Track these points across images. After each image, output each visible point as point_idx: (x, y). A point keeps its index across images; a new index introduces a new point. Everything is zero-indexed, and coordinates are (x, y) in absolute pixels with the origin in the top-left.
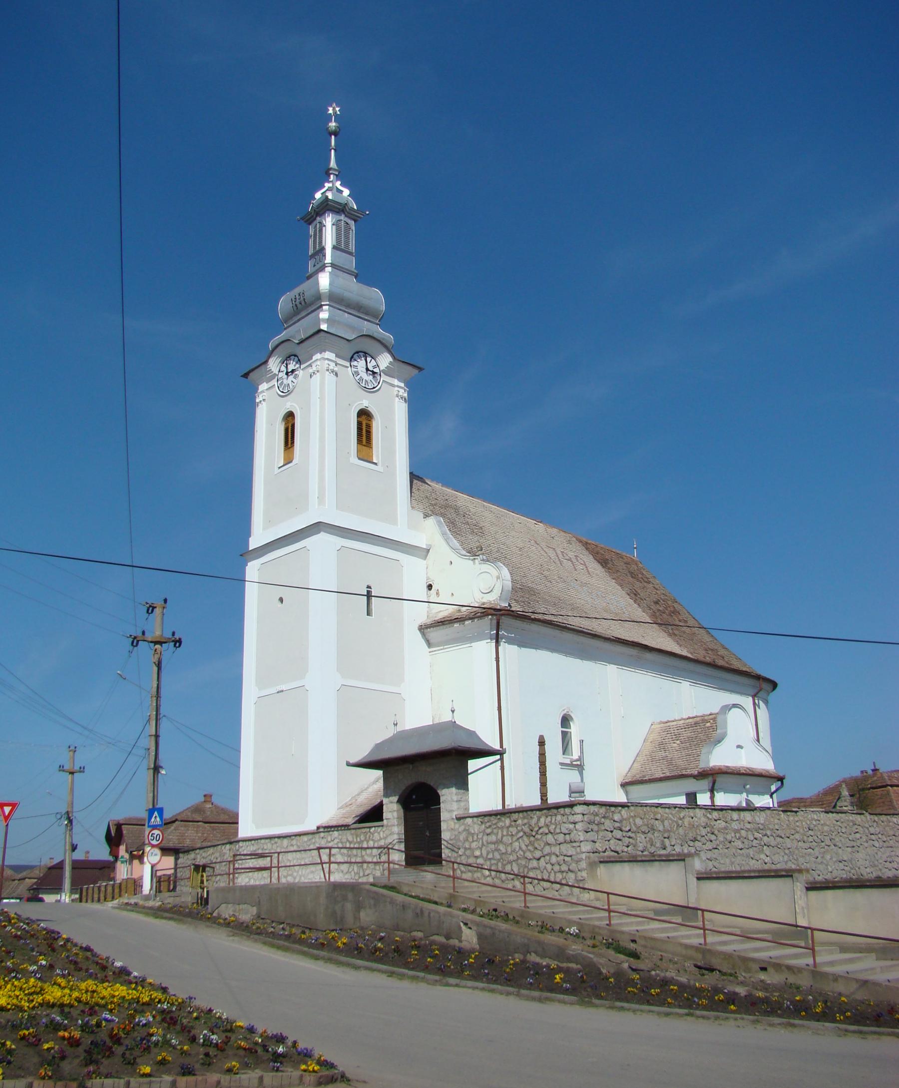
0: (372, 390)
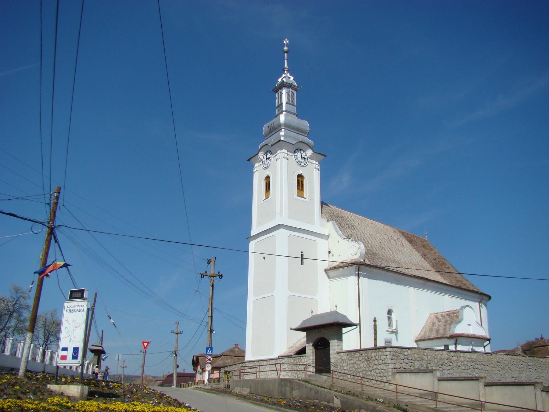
0: (304, 166)
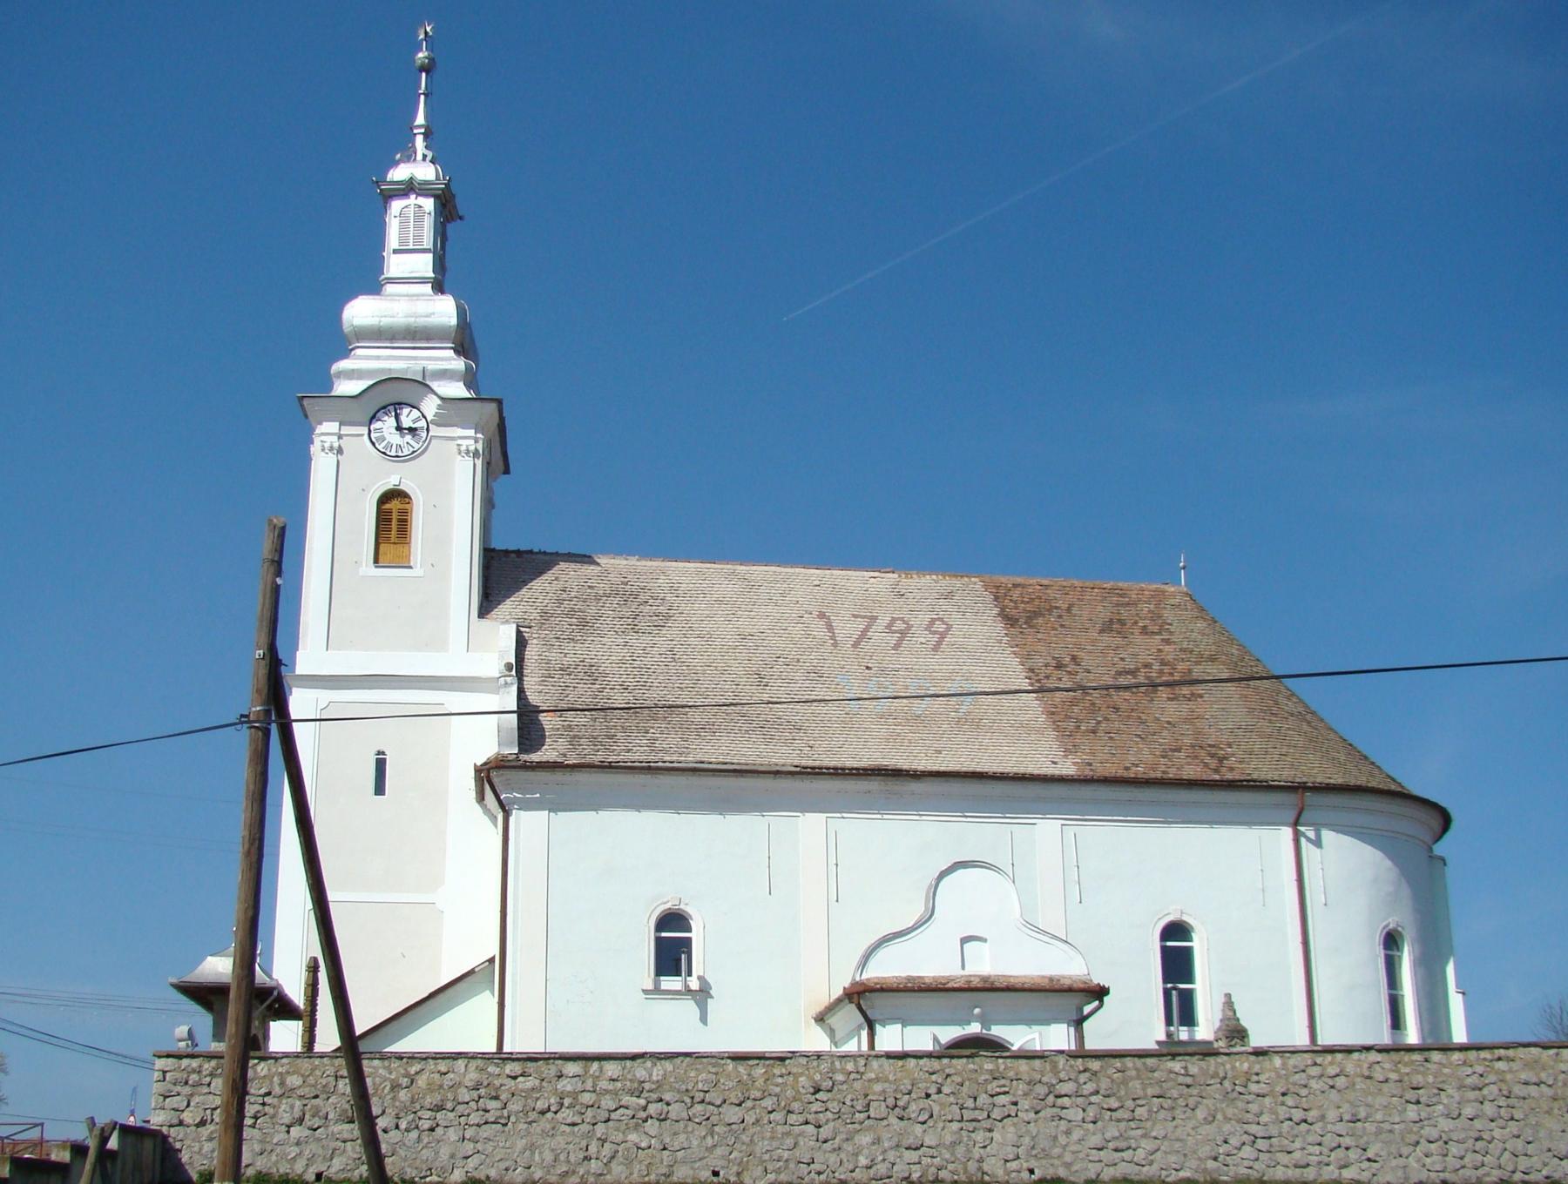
0: (414, 455)
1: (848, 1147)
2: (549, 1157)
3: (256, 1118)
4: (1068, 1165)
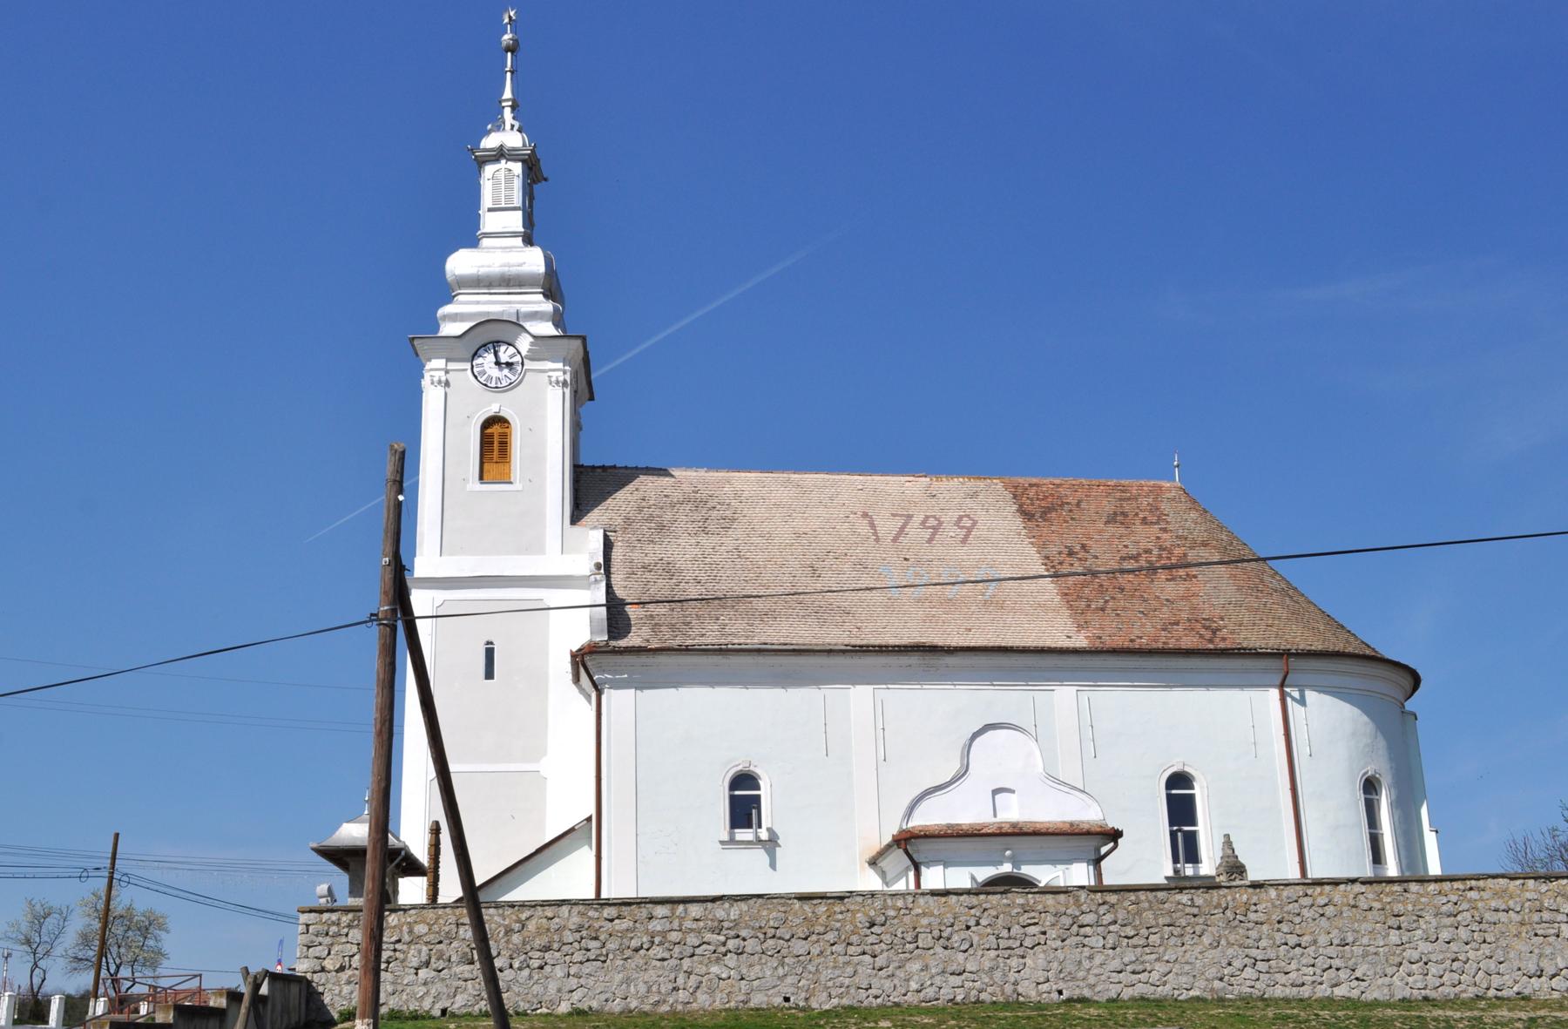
0: (511, 386)
1: (901, 974)
2: (642, 989)
3: (388, 963)
4: (1092, 986)
